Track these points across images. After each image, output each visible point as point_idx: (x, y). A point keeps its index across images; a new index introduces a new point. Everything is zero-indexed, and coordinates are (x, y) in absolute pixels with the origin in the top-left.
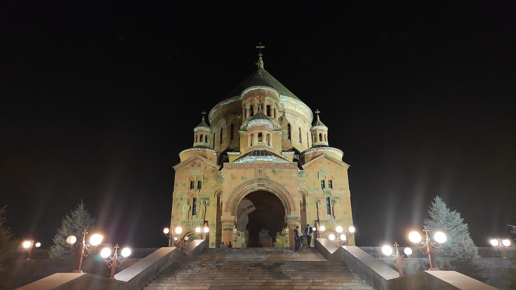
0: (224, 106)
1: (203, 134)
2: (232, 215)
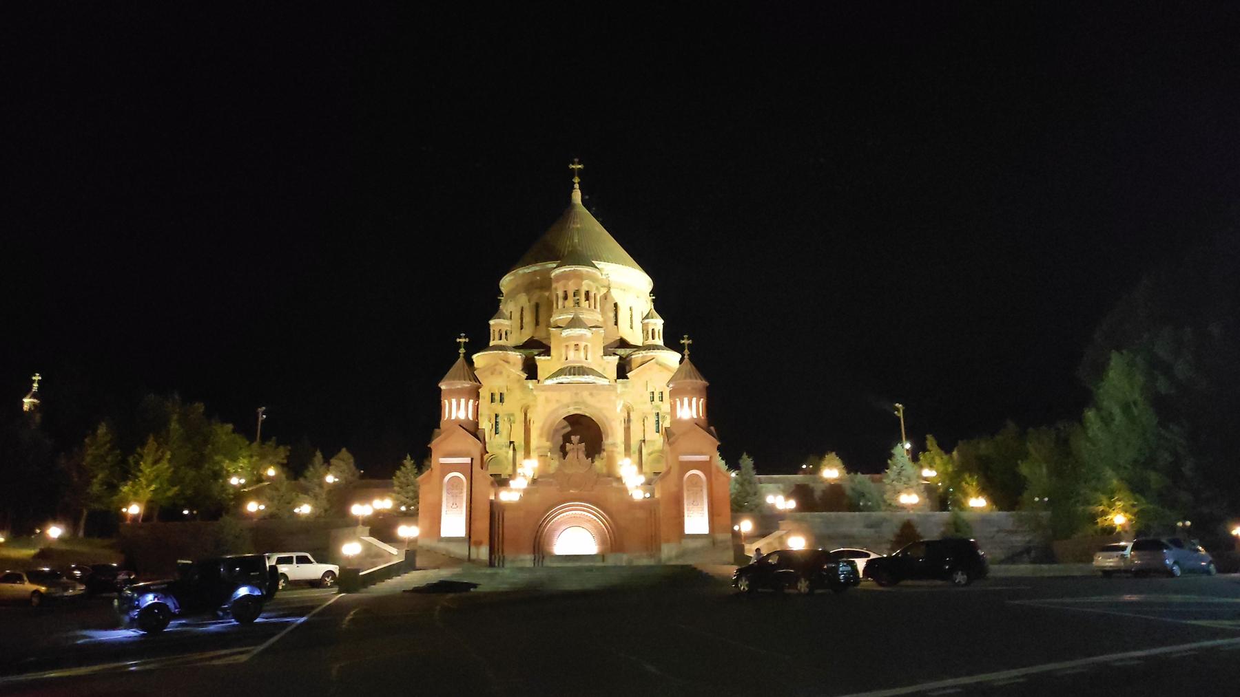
0: (525, 273)
1: (502, 330)
2: (548, 441)
